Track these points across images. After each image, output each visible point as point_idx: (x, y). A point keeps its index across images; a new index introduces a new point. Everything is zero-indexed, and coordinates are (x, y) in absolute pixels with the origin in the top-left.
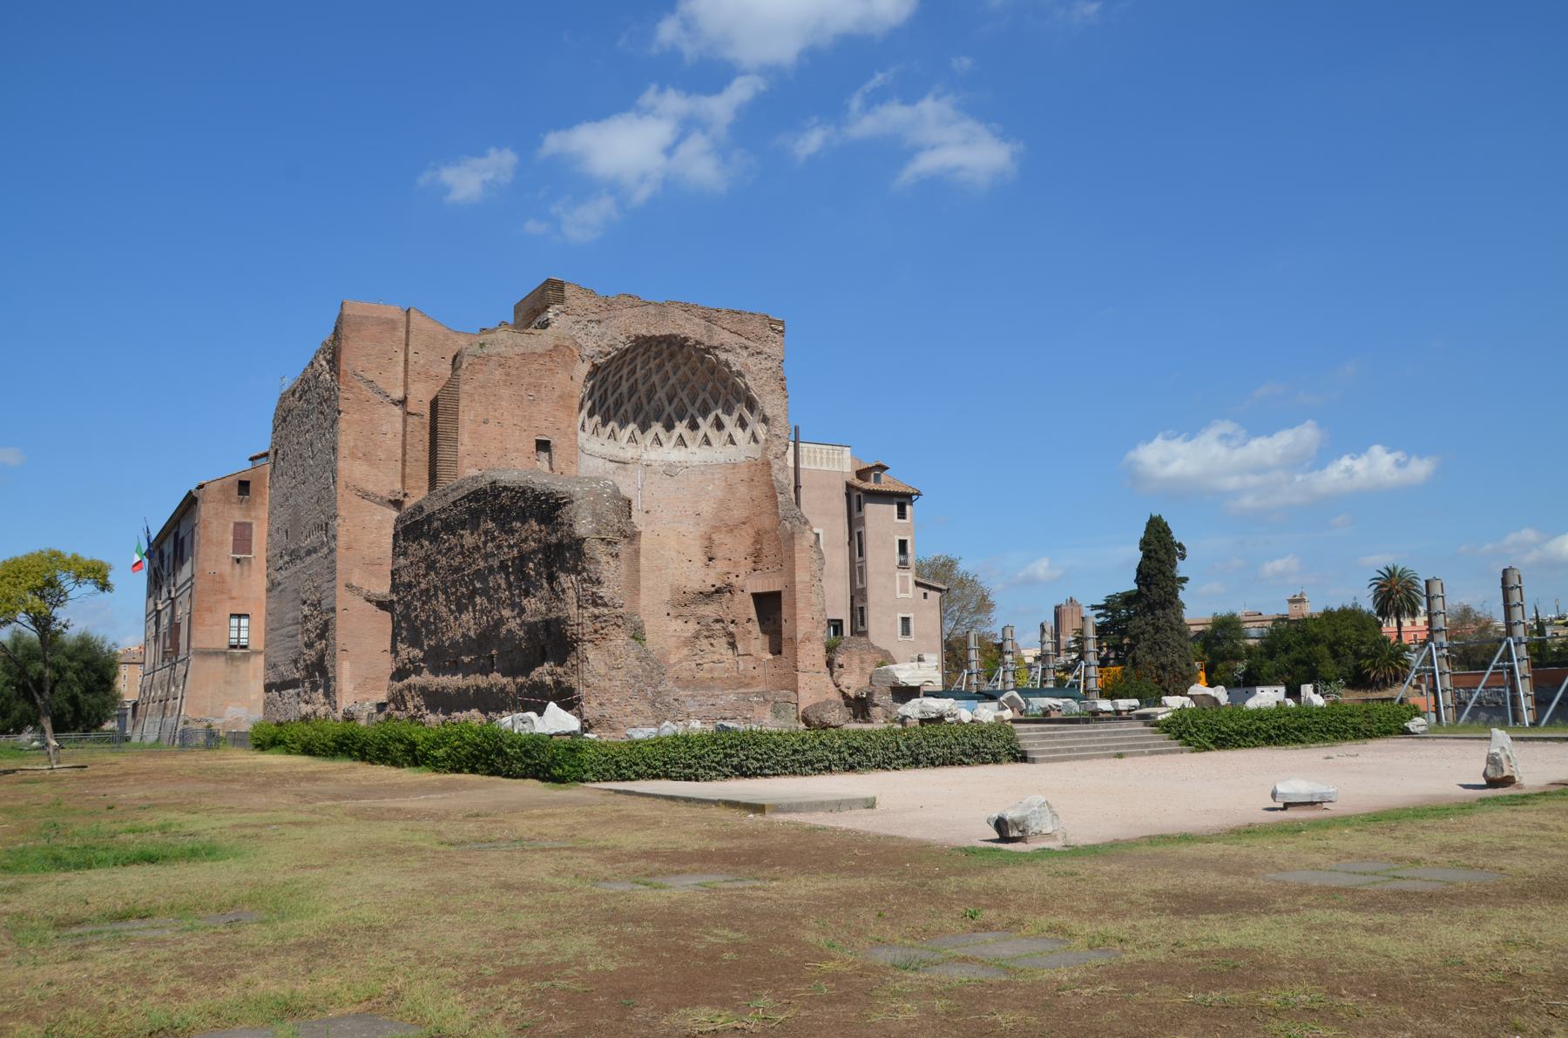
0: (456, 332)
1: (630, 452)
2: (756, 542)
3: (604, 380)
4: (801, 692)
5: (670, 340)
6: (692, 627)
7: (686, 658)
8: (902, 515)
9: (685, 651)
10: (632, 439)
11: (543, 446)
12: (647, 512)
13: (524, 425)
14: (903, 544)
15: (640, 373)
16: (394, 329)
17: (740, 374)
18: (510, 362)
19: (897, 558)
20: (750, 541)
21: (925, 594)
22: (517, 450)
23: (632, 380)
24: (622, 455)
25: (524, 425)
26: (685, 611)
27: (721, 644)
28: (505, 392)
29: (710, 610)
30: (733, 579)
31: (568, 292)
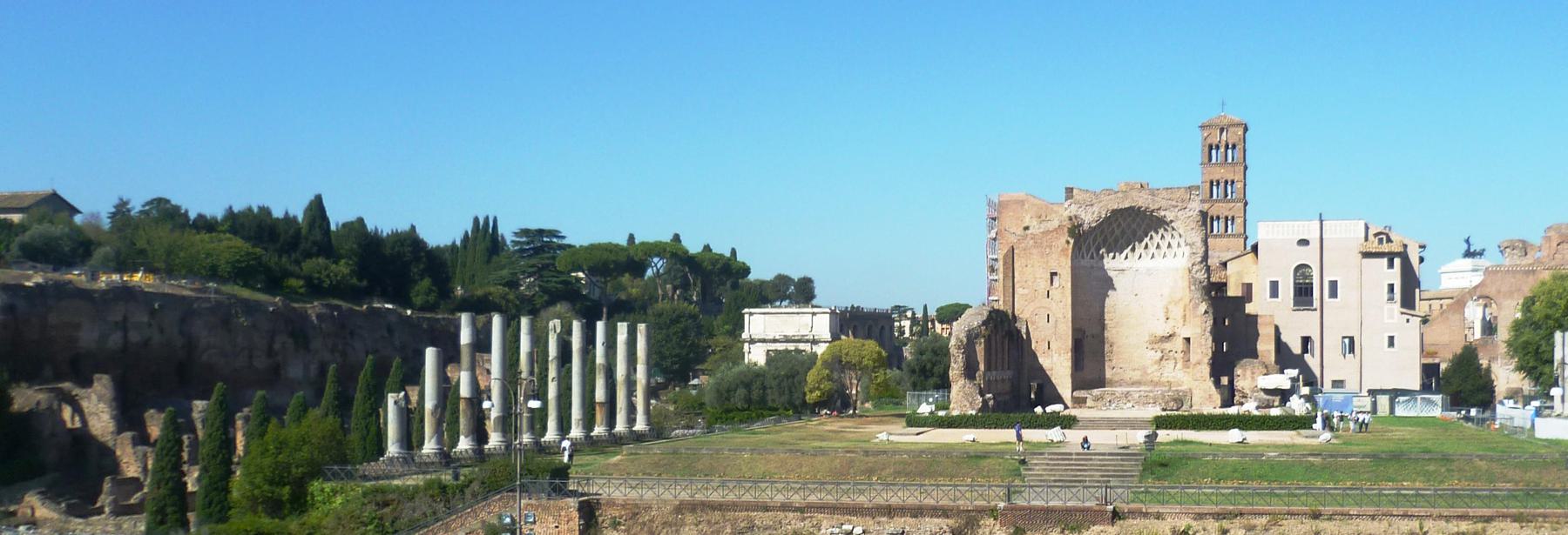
0: (1052, 204)
1: (1125, 265)
2: (1185, 311)
3: (1102, 232)
4: (1194, 391)
5: (1131, 208)
6: (1159, 354)
7: (1156, 371)
8: (1391, 265)
9: (1156, 367)
10: (1126, 258)
11: (1053, 274)
12: (1136, 295)
13: (1044, 266)
14: (1391, 287)
15: (1124, 225)
16: (1024, 205)
17: (1172, 221)
18: (1037, 237)
19: (1386, 298)
20: (1182, 310)
21: (1408, 321)
22: (1041, 278)
23: (1120, 230)
24: (1121, 267)
25: (1044, 266)
26: (1156, 346)
27: (1172, 363)
28: (1034, 251)
29: (1168, 346)
30: (1176, 330)
31: (1075, 190)
